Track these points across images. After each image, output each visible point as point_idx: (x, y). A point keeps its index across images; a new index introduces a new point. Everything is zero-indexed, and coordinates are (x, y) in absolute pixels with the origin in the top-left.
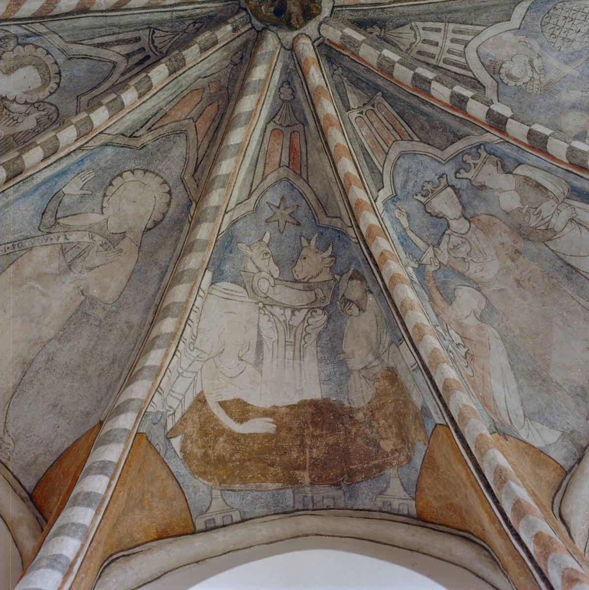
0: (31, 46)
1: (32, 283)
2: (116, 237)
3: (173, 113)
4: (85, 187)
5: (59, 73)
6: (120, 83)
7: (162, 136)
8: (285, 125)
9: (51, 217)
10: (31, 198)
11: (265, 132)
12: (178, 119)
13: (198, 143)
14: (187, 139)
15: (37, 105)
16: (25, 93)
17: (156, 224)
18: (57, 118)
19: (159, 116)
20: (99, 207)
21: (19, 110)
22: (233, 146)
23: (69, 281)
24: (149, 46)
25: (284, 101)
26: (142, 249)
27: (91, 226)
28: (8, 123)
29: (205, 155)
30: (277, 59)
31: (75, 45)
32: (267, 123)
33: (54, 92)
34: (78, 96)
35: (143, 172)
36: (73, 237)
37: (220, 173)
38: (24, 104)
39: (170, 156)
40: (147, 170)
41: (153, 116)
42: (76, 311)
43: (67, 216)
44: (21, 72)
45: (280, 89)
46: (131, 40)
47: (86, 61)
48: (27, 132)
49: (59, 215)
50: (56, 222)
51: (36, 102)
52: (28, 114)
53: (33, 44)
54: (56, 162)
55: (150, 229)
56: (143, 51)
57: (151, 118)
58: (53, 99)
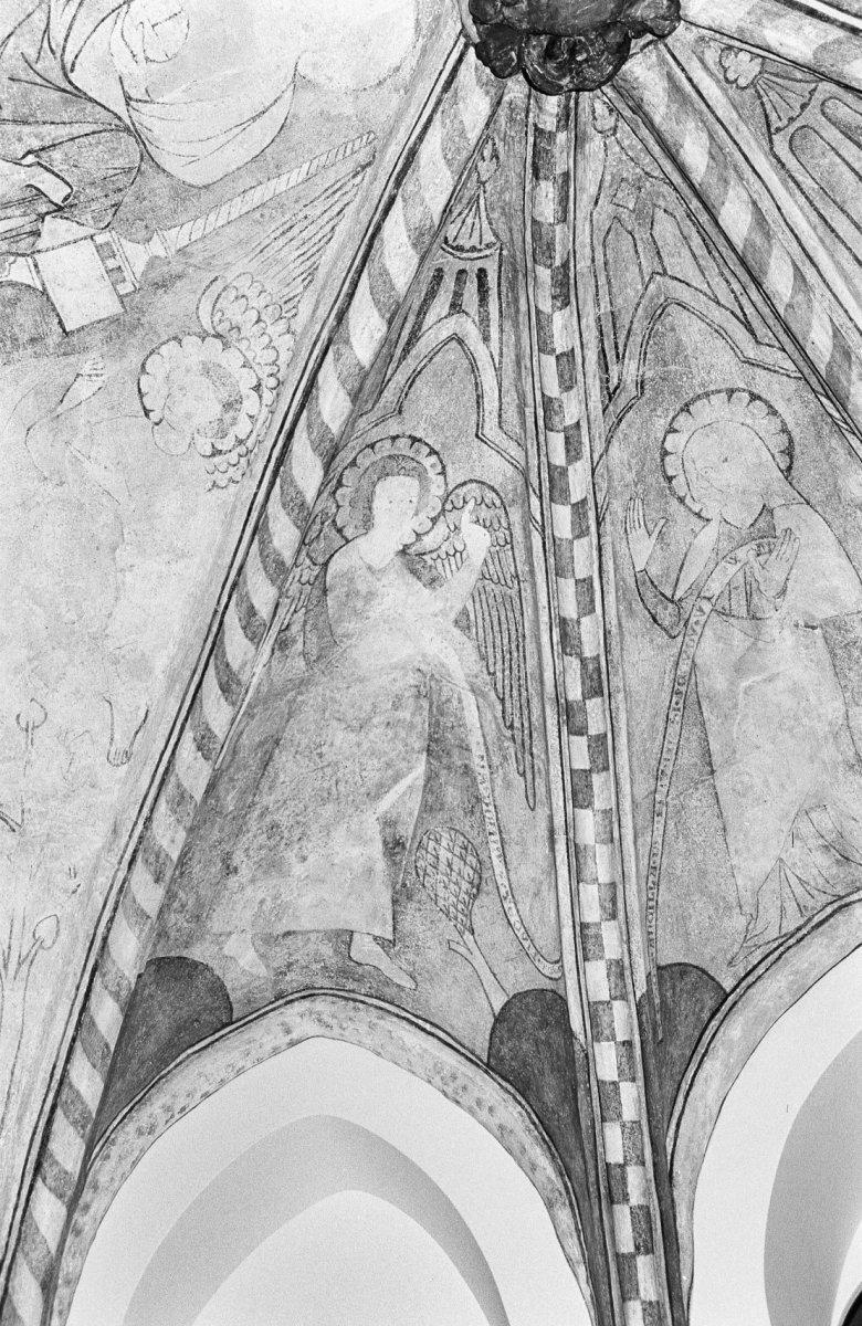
0: (346, 472)
1: (744, 684)
2: (761, 524)
3: (619, 301)
4: (651, 526)
5: (414, 440)
6: (501, 355)
7: (645, 344)
8: (798, 111)
9: (666, 609)
10: (628, 638)
11: (783, 165)
12: (636, 300)
13: (705, 294)
14: (684, 308)
15: (448, 504)
16: (416, 514)
17: (789, 452)
18: (498, 494)
19: (608, 328)
20: (694, 519)
21: (439, 539)
22: (795, 291)
23: (775, 632)
24: (462, 259)
25: (753, 84)
26: (813, 501)
27: (716, 551)
28: (454, 567)
29: (736, 297)
30: (683, 70)
31: (385, 393)
32: (771, 149)
33: (444, 467)
34: (477, 436)
35: (684, 413)
36: (715, 587)
37: (827, 359)
38: (434, 524)
39: (689, 352)
40: (686, 405)
41: (602, 341)
42: (834, 655)
43: (678, 580)
44: (379, 504)
45: (727, 80)
46: (433, 288)
47: (418, 381)
48: (494, 556)
49: (669, 594)
50: (677, 603)
51: (443, 505)
52: (456, 528)
53: (346, 468)
54: (601, 578)
55: (790, 468)
56: (464, 275)
57: (603, 344)
58: (455, 477)
